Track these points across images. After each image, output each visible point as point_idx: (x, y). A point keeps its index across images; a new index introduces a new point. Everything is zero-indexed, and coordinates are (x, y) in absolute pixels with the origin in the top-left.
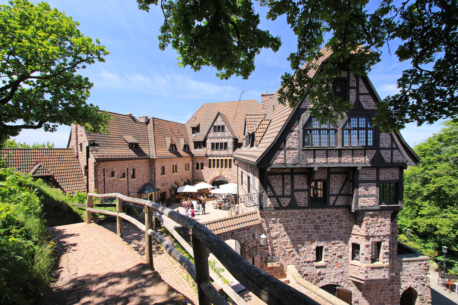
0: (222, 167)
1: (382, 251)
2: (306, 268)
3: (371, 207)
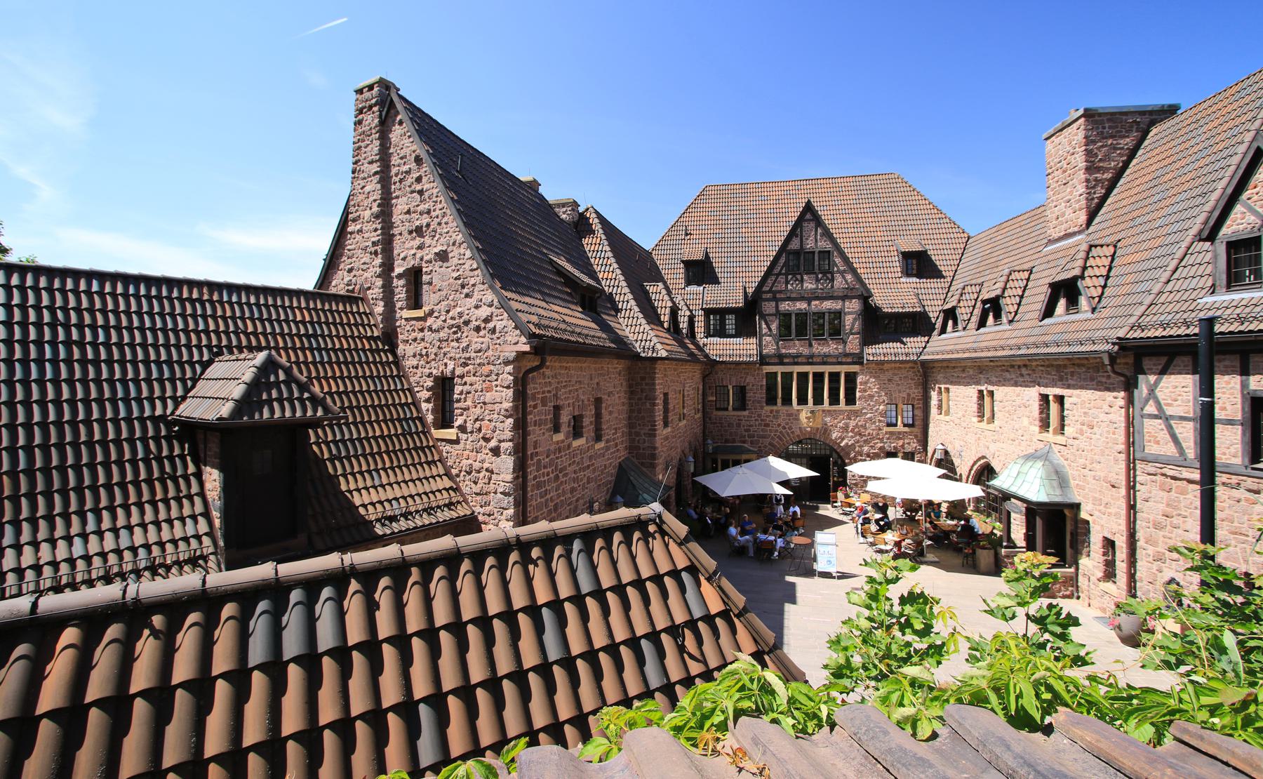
0: (818, 400)
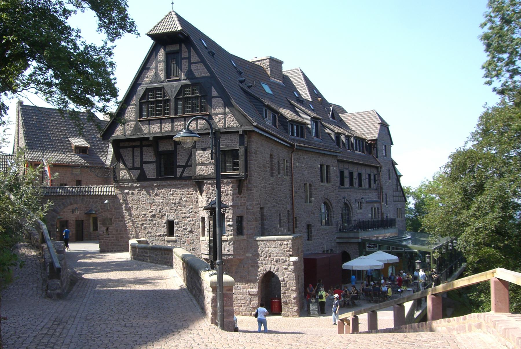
3: (210, 175)
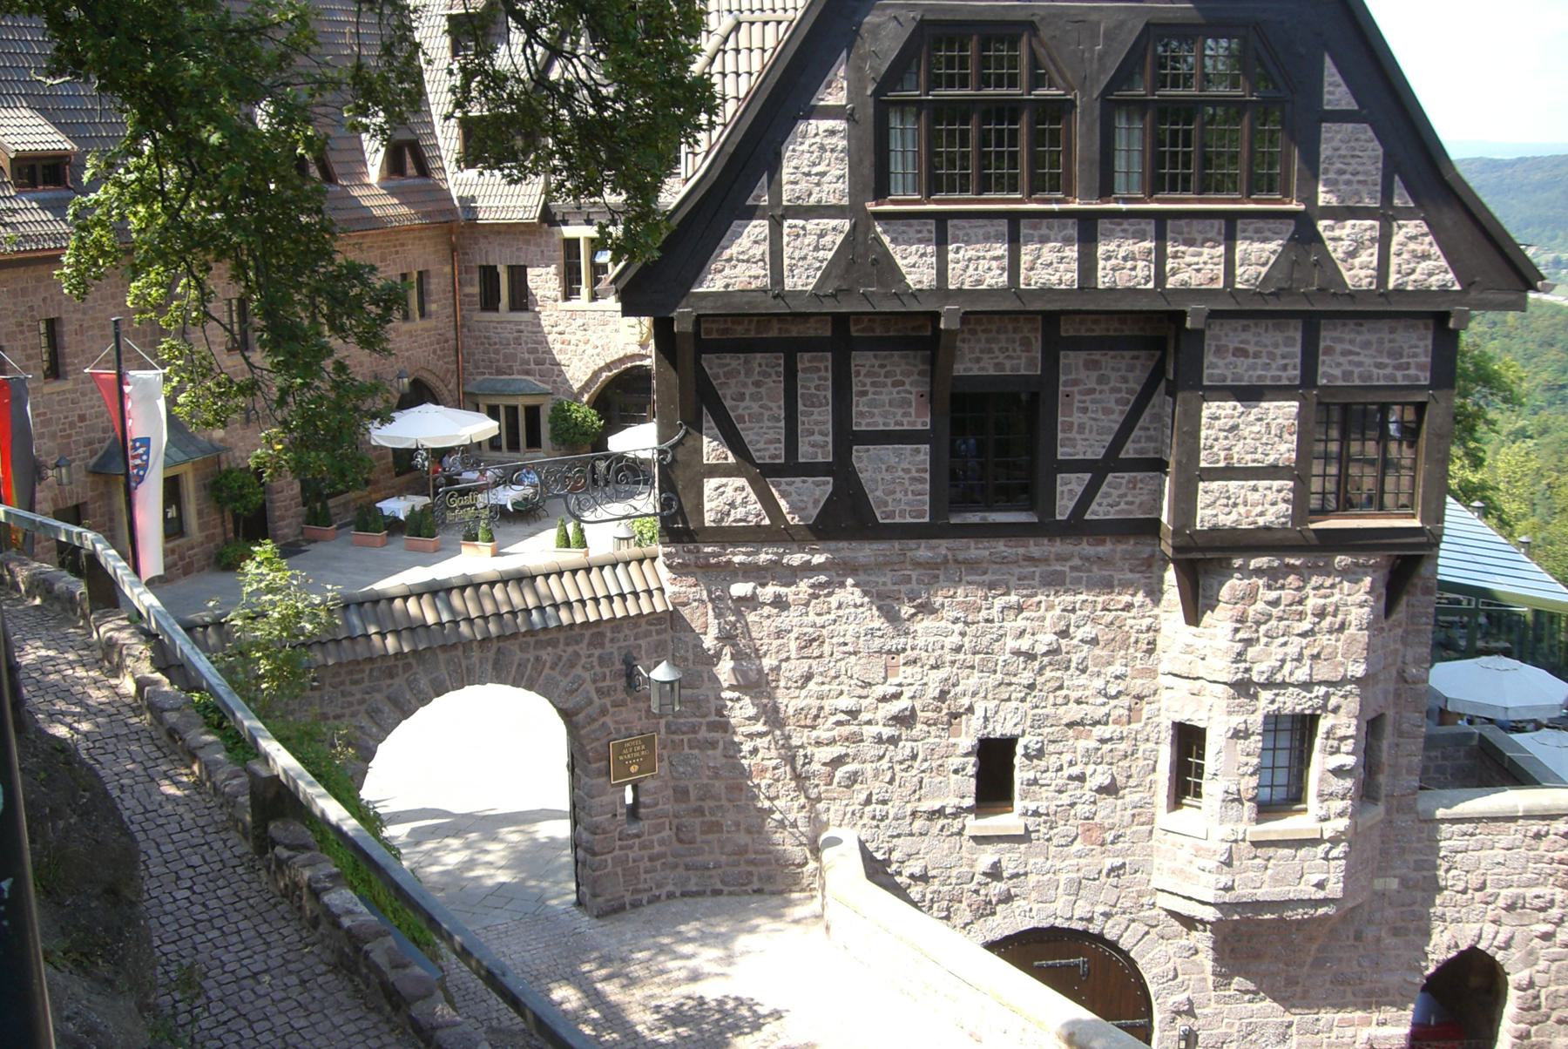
1: (1320, 763)
2: (924, 844)
3: (1267, 529)
